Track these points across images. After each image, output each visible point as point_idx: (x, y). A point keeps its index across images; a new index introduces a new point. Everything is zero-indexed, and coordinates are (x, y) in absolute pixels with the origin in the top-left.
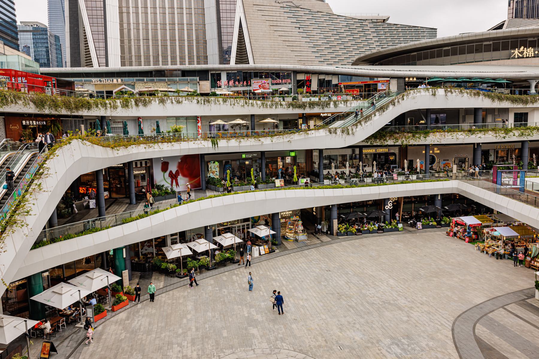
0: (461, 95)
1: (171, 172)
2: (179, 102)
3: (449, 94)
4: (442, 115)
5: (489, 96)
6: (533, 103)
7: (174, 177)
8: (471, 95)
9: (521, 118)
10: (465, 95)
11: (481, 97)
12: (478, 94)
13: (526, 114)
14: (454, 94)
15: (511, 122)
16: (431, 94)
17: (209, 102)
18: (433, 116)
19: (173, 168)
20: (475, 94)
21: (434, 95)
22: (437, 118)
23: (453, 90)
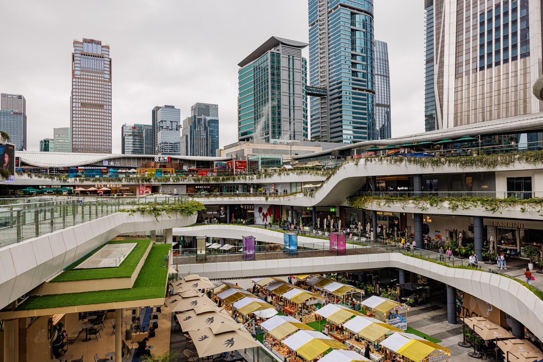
0: (380, 162)
1: (263, 213)
2: (288, 174)
3: (368, 163)
4: (434, 181)
5: (416, 162)
6: (507, 164)
7: (265, 216)
8: (391, 161)
9: (520, 186)
10: (385, 162)
11: (404, 163)
12: (401, 160)
13: (531, 177)
14: (374, 162)
15: (501, 189)
16: (355, 162)
17: (301, 173)
18: (428, 182)
19: (265, 211)
20: (396, 161)
21: (357, 164)
22: (431, 183)
23: (373, 159)
